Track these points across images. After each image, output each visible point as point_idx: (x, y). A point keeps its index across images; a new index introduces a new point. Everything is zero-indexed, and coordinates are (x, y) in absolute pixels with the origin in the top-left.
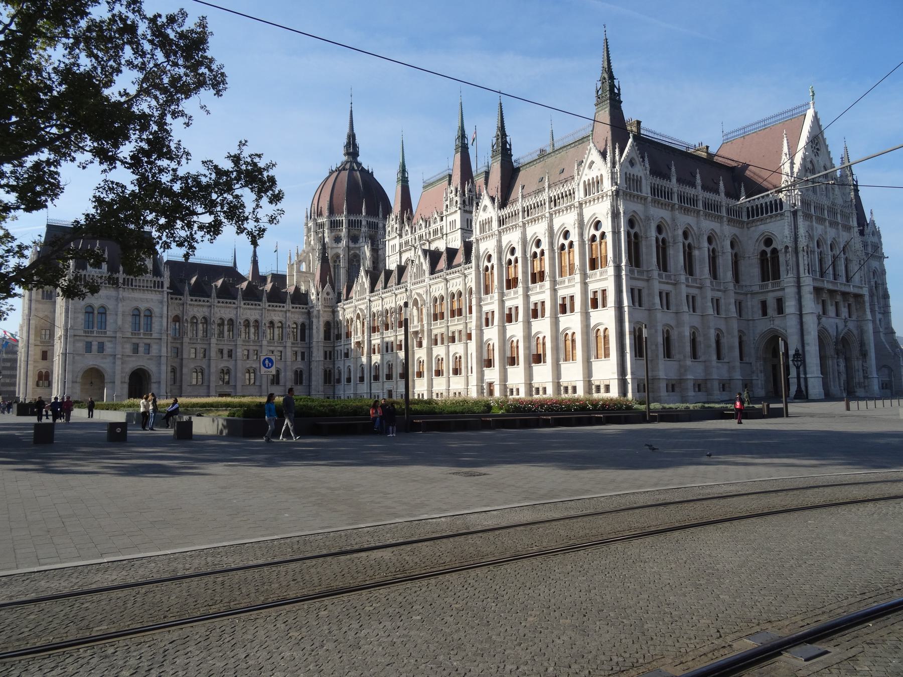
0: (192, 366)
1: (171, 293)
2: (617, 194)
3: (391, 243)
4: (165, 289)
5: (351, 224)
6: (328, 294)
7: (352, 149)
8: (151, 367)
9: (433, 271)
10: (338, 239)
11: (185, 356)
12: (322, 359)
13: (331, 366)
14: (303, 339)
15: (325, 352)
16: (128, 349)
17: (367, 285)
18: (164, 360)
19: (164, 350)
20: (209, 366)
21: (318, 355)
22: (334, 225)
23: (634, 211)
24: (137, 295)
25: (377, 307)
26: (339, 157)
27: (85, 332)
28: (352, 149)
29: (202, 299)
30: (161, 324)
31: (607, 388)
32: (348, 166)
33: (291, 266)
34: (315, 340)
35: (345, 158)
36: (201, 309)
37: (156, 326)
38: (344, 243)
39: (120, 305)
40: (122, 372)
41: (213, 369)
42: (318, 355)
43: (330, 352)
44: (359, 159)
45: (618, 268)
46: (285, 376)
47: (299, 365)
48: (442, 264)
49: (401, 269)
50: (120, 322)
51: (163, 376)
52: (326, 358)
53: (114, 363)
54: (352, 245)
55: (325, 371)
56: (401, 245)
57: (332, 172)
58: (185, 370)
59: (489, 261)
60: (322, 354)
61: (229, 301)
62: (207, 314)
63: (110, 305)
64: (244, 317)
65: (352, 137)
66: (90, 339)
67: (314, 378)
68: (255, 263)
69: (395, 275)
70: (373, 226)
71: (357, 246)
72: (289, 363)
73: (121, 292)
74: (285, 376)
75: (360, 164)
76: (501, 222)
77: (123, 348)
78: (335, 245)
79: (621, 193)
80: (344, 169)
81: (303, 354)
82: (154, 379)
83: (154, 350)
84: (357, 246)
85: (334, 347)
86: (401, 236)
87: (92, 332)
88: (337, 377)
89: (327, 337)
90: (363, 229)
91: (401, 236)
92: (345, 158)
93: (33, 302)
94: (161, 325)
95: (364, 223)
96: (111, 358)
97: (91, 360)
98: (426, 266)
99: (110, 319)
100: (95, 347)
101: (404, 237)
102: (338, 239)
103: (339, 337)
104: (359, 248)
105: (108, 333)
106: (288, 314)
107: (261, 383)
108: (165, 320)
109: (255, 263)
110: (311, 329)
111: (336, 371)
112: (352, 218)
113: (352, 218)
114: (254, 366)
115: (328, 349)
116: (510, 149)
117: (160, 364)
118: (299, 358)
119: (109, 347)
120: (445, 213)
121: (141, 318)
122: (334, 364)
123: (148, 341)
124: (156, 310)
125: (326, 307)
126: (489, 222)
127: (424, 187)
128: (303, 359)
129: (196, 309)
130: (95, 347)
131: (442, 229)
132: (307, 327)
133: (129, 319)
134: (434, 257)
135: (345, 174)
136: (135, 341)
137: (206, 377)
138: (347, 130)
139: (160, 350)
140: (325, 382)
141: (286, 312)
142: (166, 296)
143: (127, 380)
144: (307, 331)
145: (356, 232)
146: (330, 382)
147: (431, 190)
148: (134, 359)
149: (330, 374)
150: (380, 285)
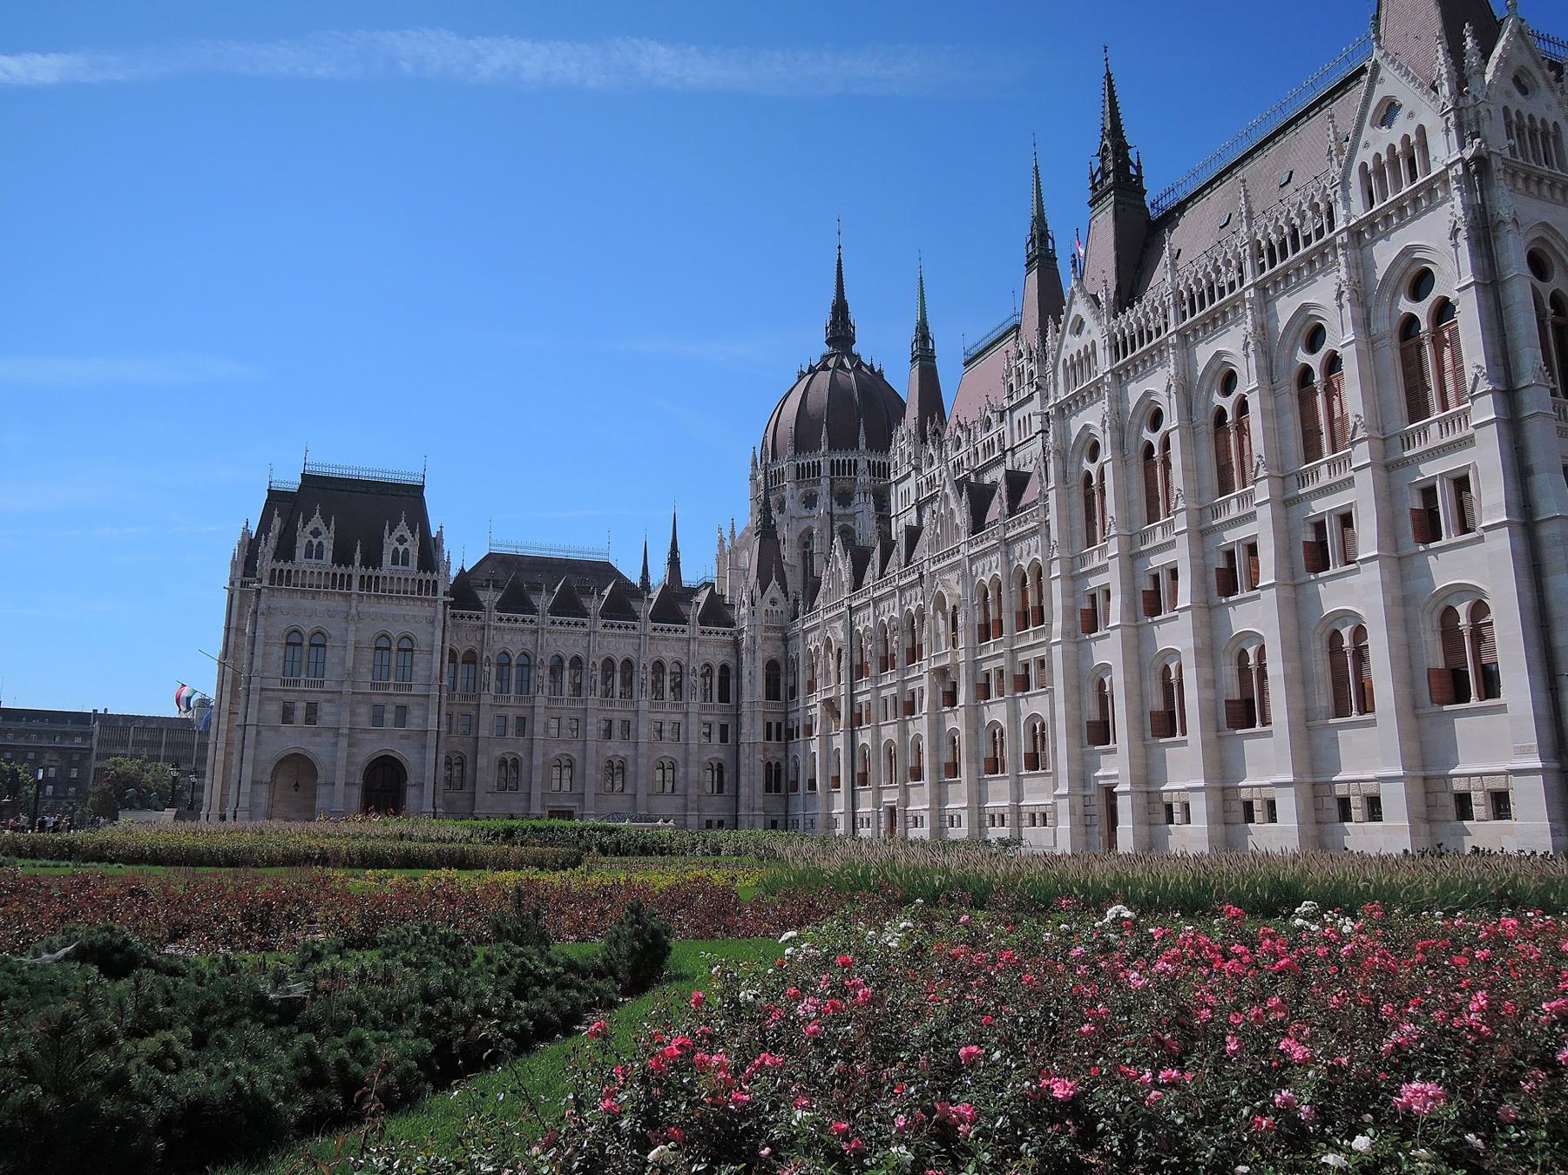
0: (498, 753)
1: (451, 603)
2: (1478, 171)
3: (902, 487)
4: (440, 594)
6: (773, 602)
7: (841, 332)
9: (978, 523)
10: (810, 501)
11: (483, 732)
12: (761, 738)
13: (781, 755)
14: (724, 697)
15: (769, 725)
16: (364, 716)
17: (846, 576)
18: (431, 740)
19: (433, 718)
20: (531, 754)
21: (752, 731)
22: (806, 474)
23: (1545, 225)
24: (384, 607)
25: (865, 622)
26: (816, 346)
27: (283, 682)
28: (841, 332)
29: (521, 616)
30: (428, 666)
31: (1500, 804)
32: (831, 363)
33: (720, 558)
34: (746, 698)
35: (827, 349)
36: (518, 637)
37: (420, 670)
38: (821, 510)
40: (349, 763)
41: (538, 760)
43: (779, 725)
44: (855, 349)
45: (1509, 396)
46: (686, 774)
47: (716, 751)
48: (997, 508)
49: (913, 534)
50: (349, 664)
51: (430, 772)
52: (769, 738)
53: (335, 744)
54: (838, 510)
55: (769, 765)
56: (919, 488)
57: (801, 376)
58: (482, 761)
59: (1093, 458)
60: (760, 729)
61: (573, 620)
62: (530, 646)
63: (334, 629)
64: (604, 653)
65: (840, 309)
66: (290, 697)
67: (743, 780)
68: (674, 562)
69: (902, 545)
70: (882, 471)
71: (849, 511)
72: (693, 747)
73: (354, 603)
74: (686, 774)
75: (858, 357)
76: (1119, 347)
77: (353, 713)
78: (805, 513)
79: (1496, 163)
80: (825, 368)
81: (724, 728)
82: (411, 780)
83: (414, 720)
84: (849, 511)
85: (787, 713)
86: (918, 469)
87: (297, 682)
89: (772, 692)
90: (860, 479)
91: (918, 469)
92: (827, 349)
93: (233, 632)
94: (430, 669)
95: (862, 465)
96: (331, 734)
97: (292, 739)
98: (962, 517)
99: (332, 656)
100: (300, 713)
101: (926, 471)
102: (810, 501)
103: (793, 692)
104: (853, 516)
105: (327, 686)
106: (694, 646)
107: (636, 788)
108: (437, 657)
109: (674, 562)
110: (739, 676)
111: (791, 764)
112: (838, 457)
113: (838, 457)
114: (621, 753)
115: (774, 720)
116: (1139, 177)
117: (424, 747)
118: (716, 737)
119: (327, 712)
121: (392, 651)
122: (786, 750)
123: (401, 701)
124: (422, 638)
125: (768, 629)
126: (1089, 355)
127: (967, 364)
128: (724, 739)
129: (507, 637)
130: (300, 713)
132: (733, 672)
133: (369, 655)
134: (979, 498)
135: (824, 378)
136: (378, 700)
137: (524, 774)
139: (426, 720)
140: (768, 789)
141: (688, 640)
142: (441, 608)
143: (359, 780)
144: (732, 682)
145: (847, 485)
146: (778, 790)
147: (981, 365)
148: (373, 736)
149: (778, 772)
150: (872, 571)
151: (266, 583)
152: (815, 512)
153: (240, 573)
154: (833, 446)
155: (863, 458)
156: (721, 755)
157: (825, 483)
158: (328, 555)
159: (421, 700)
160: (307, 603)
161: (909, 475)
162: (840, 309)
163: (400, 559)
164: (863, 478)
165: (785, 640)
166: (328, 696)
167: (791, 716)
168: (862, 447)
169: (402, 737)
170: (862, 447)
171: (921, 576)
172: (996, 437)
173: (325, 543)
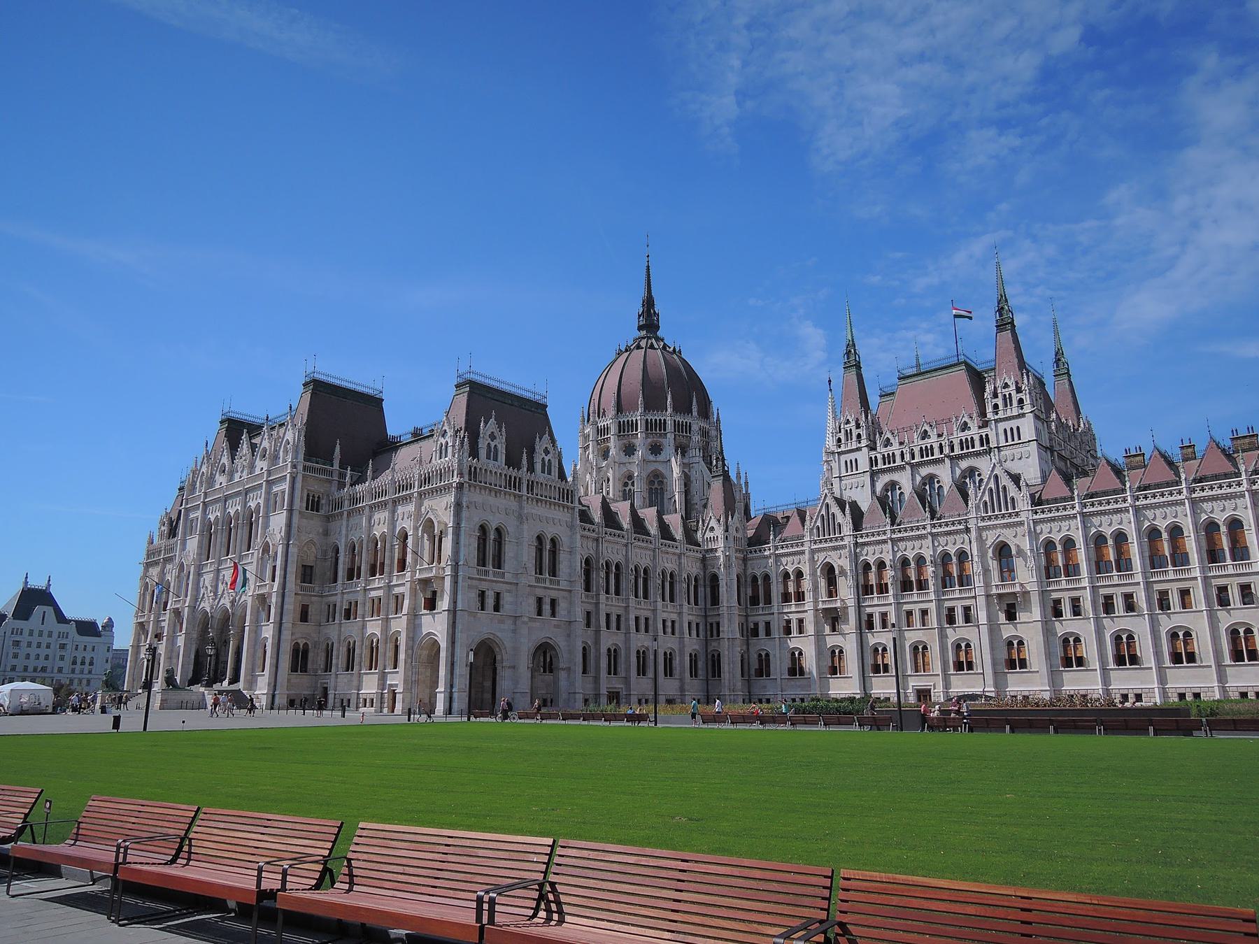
5: (678, 426)
7: (649, 323)
8: (560, 642)
14: (696, 604)
21: (730, 628)
26: (630, 331)
30: (571, 566)
39: (525, 527)
42: (730, 628)
56: (873, 462)
63: (511, 527)
65: (649, 303)
78: (652, 458)
81: (697, 624)
88: (755, 665)
91: (872, 448)
95: (695, 427)
112: (679, 418)
113: (679, 418)
117: (569, 636)
118: (694, 632)
120: (990, 416)
122: (748, 645)
124: (564, 540)
131: (985, 440)
132: (701, 582)
138: (641, 293)
144: (701, 589)
151: (466, 478)
152: (661, 458)
153: (301, 456)
154: (676, 409)
155: (697, 424)
156: (697, 647)
157: (670, 436)
158: (502, 457)
159: (566, 594)
160: (491, 500)
161: (859, 449)
162: (649, 303)
163: (546, 468)
164: (696, 438)
165: (745, 560)
166: (508, 587)
167: (750, 619)
168: (695, 414)
169: (555, 626)
170: (695, 414)
171: (967, 530)
172: (977, 438)
173: (499, 446)
